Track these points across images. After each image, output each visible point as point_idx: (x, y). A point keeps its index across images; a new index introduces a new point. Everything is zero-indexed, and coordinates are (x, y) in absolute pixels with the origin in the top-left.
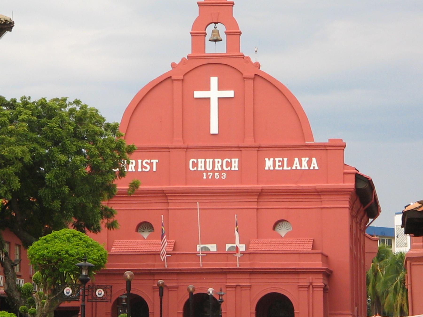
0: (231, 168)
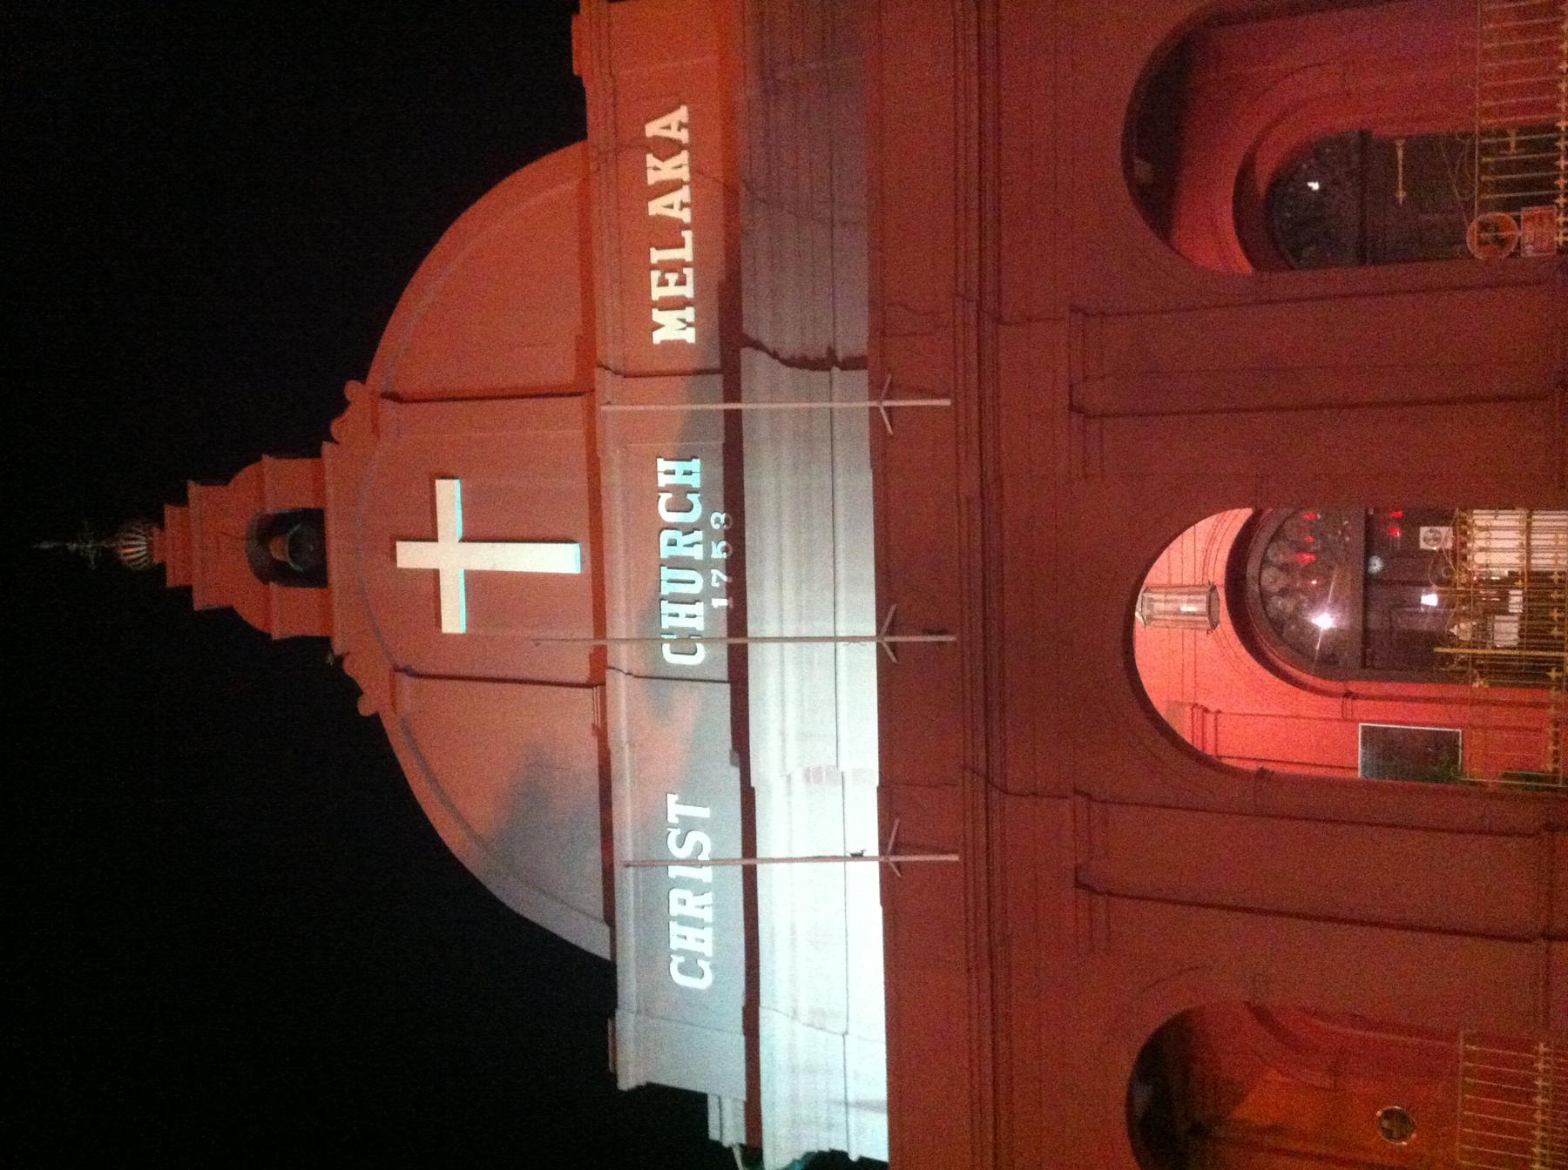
0: (694, 491)
